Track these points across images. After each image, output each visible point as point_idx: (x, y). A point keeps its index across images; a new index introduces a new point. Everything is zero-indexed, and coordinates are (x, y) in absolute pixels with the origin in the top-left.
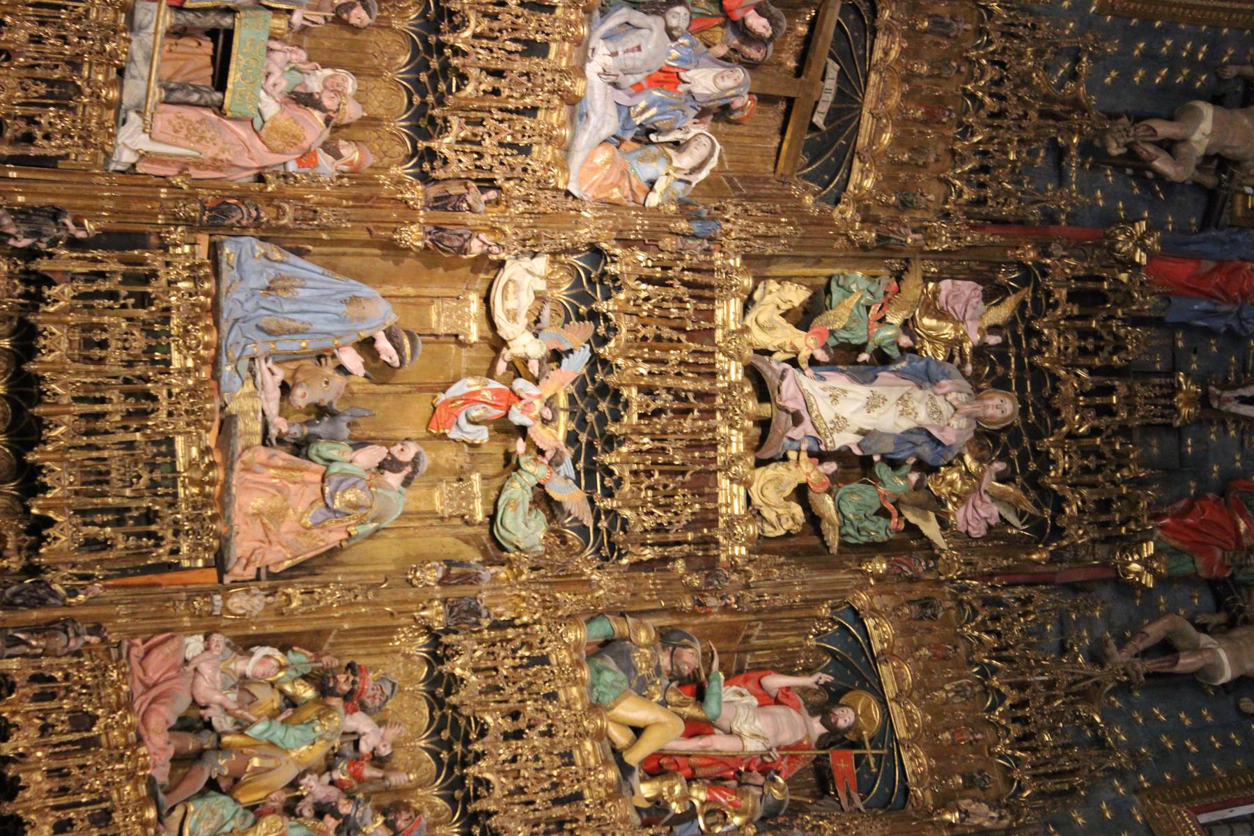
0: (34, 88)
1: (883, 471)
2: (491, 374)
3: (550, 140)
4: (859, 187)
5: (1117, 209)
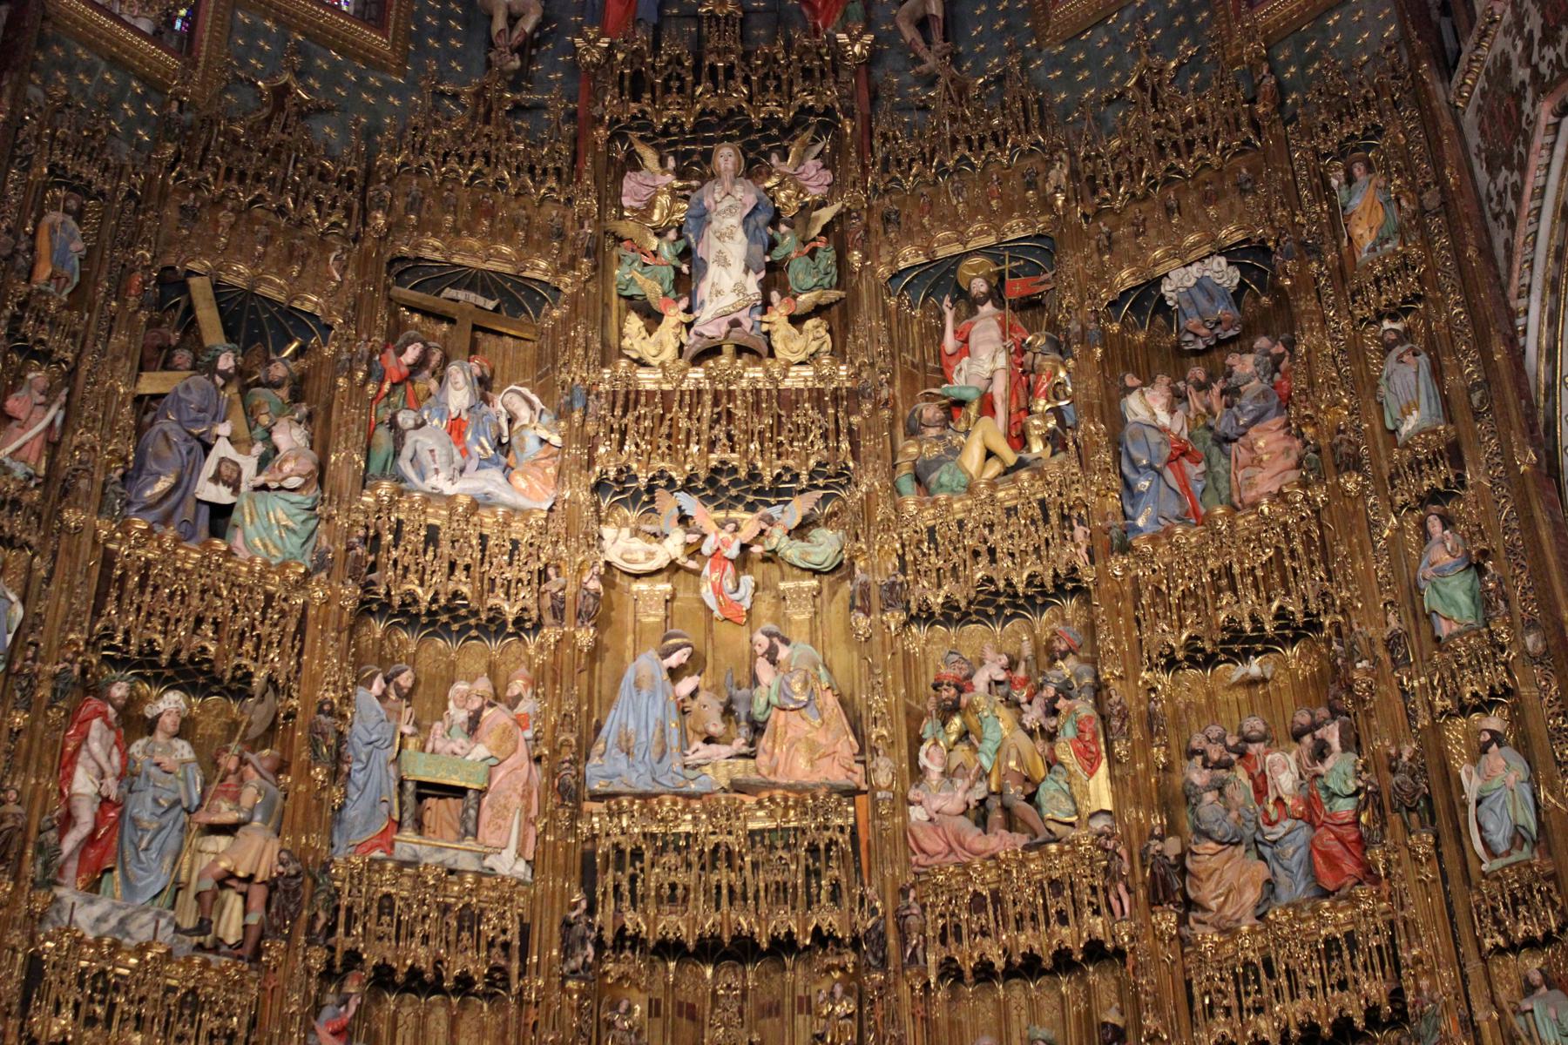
1: (778, 254)
2: (697, 573)
3: (506, 524)
4: (545, 271)
5: (565, 62)
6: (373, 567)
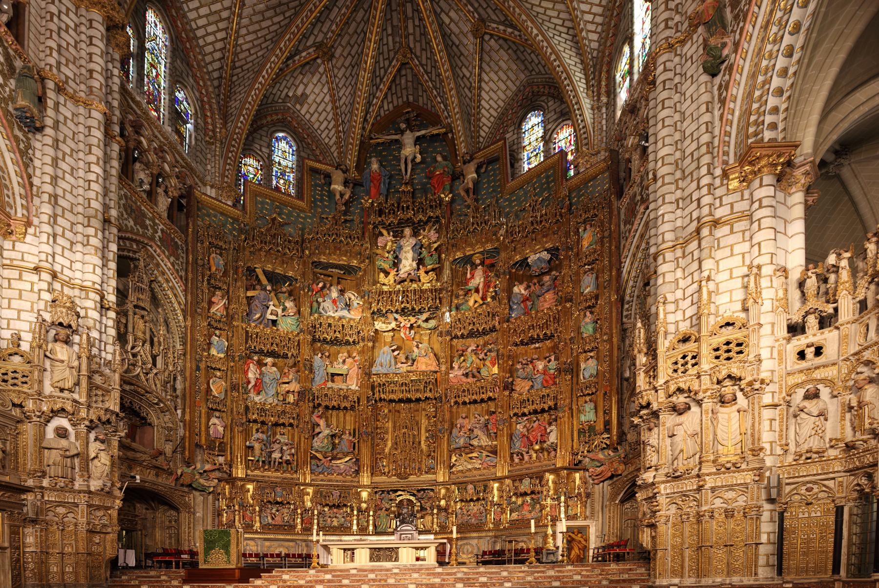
1: (422, 256)
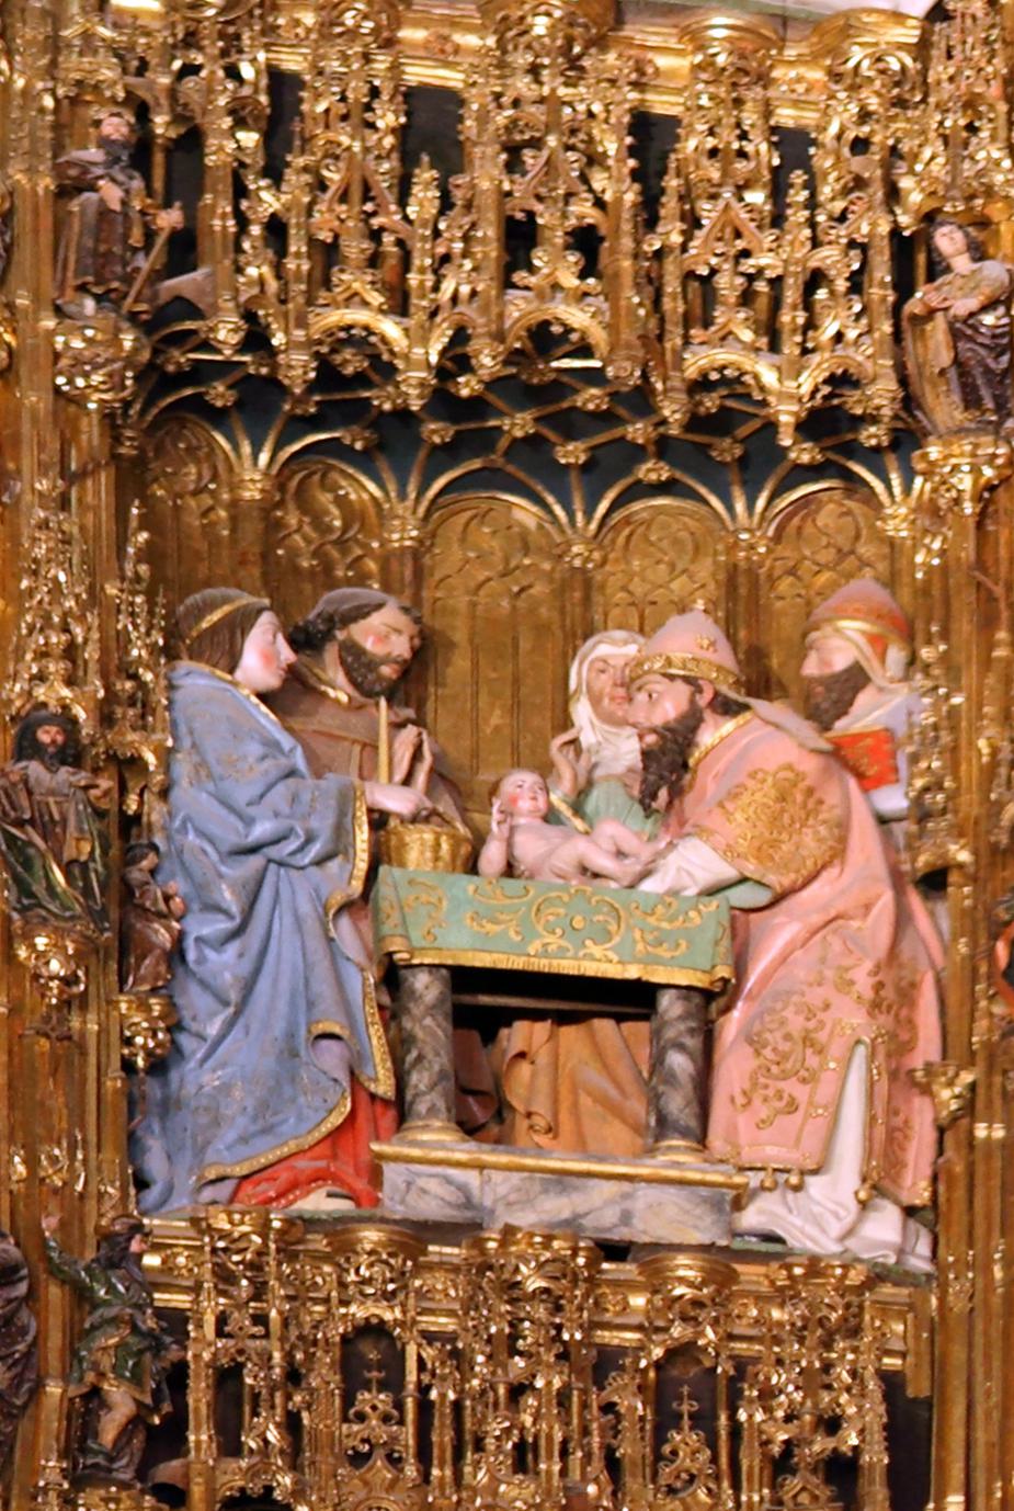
0: (684, 1460)
6: (184, 250)
